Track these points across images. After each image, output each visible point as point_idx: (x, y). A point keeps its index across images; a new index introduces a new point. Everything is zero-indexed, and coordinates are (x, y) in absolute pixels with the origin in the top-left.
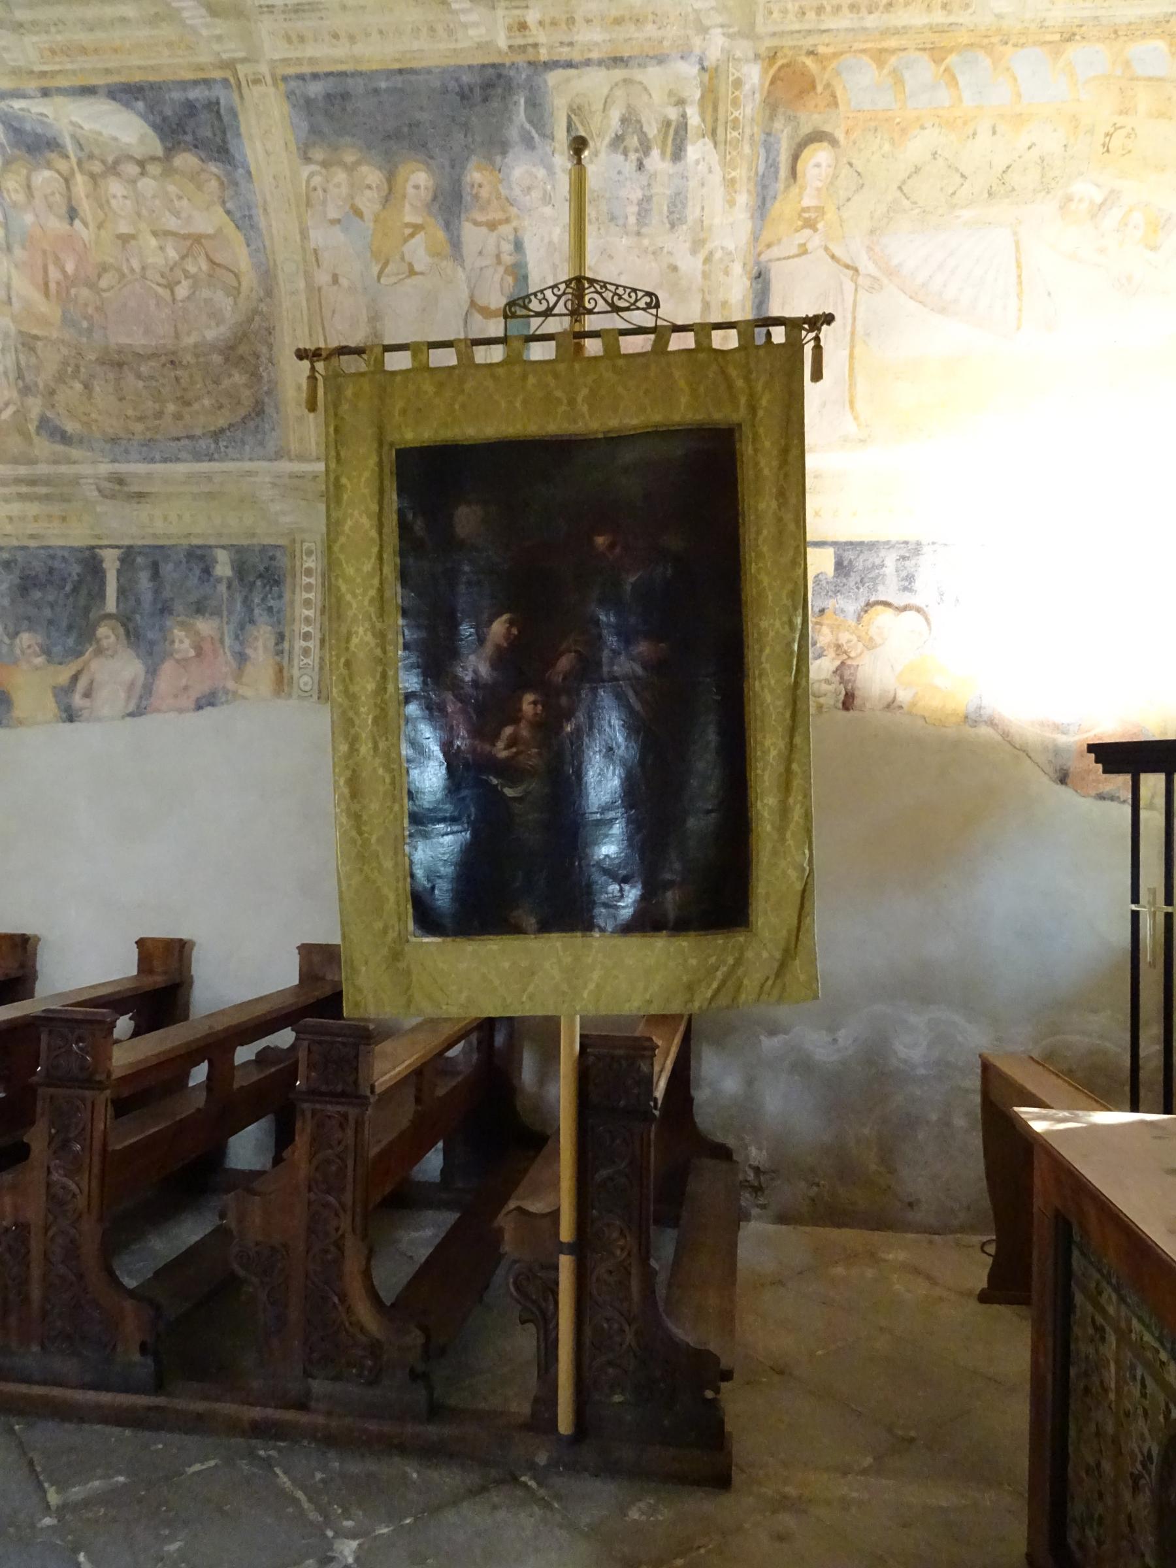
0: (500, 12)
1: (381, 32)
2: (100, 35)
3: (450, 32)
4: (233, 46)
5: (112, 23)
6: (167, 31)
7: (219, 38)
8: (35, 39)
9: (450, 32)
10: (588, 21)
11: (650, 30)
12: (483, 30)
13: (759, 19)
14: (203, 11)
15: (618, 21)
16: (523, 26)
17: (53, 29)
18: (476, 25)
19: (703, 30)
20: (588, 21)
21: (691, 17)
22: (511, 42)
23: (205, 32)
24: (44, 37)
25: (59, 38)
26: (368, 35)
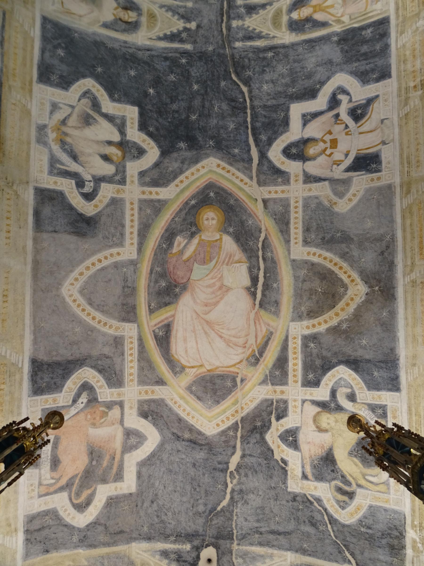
0: (411, 95)
1: (416, 134)
2: (416, 235)
3: (416, 111)
4: (420, 187)
5: (412, 229)
6: (415, 209)
7: (417, 191)
8: (417, 260)
9: (416, 111)
10: (414, 66)
11: (417, 46)
12: (416, 100)
13: (414, 13)
14: (409, 196)
15: (414, 56)
16: (415, 87)
17: (414, 252)
18: (414, 102)
19: (417, 29)
20: (414, 66)
21: (413, 34)
22: (420, 89)
23: (416, 196)
24: (416, 256)
25: (416, 250)
26: (417, 138)
